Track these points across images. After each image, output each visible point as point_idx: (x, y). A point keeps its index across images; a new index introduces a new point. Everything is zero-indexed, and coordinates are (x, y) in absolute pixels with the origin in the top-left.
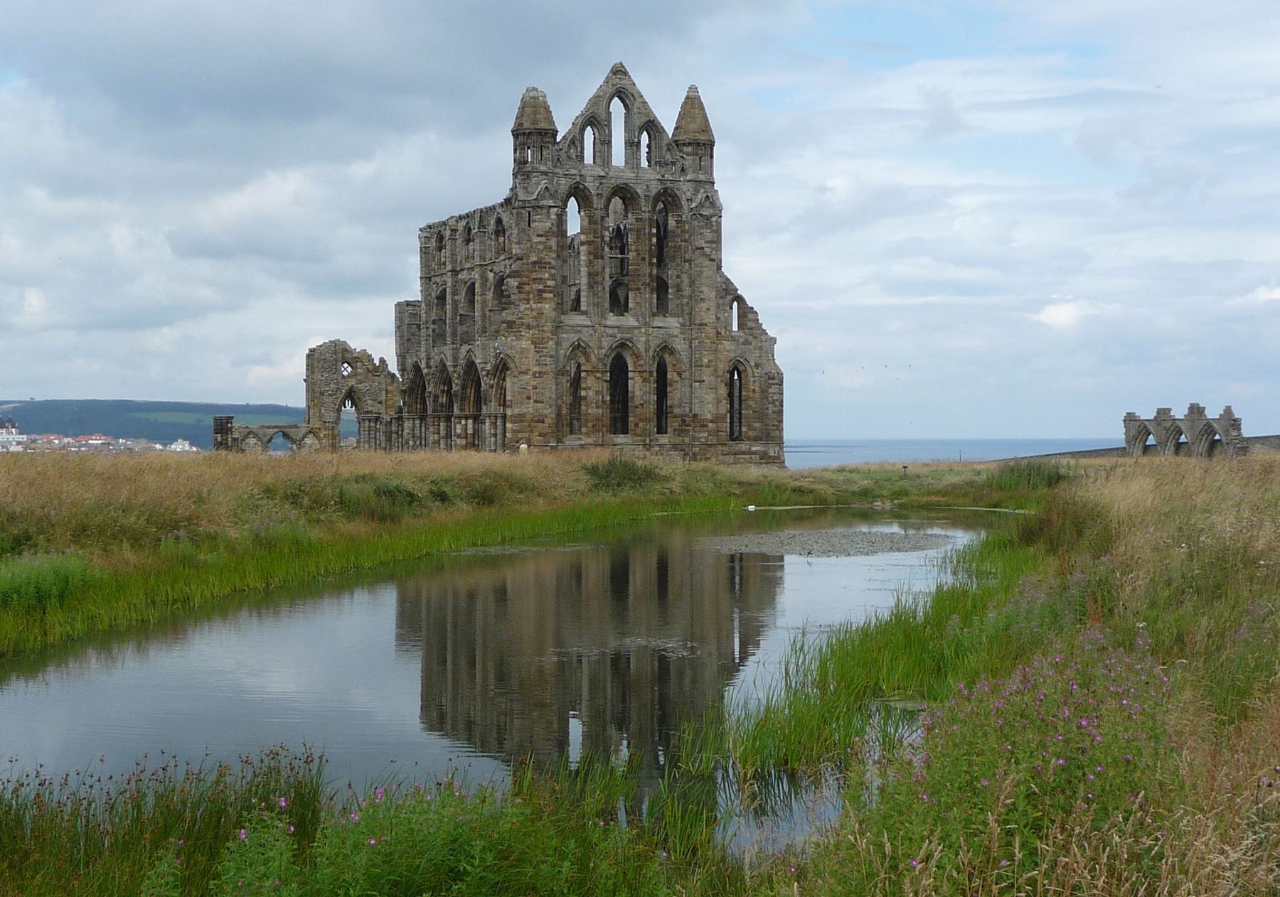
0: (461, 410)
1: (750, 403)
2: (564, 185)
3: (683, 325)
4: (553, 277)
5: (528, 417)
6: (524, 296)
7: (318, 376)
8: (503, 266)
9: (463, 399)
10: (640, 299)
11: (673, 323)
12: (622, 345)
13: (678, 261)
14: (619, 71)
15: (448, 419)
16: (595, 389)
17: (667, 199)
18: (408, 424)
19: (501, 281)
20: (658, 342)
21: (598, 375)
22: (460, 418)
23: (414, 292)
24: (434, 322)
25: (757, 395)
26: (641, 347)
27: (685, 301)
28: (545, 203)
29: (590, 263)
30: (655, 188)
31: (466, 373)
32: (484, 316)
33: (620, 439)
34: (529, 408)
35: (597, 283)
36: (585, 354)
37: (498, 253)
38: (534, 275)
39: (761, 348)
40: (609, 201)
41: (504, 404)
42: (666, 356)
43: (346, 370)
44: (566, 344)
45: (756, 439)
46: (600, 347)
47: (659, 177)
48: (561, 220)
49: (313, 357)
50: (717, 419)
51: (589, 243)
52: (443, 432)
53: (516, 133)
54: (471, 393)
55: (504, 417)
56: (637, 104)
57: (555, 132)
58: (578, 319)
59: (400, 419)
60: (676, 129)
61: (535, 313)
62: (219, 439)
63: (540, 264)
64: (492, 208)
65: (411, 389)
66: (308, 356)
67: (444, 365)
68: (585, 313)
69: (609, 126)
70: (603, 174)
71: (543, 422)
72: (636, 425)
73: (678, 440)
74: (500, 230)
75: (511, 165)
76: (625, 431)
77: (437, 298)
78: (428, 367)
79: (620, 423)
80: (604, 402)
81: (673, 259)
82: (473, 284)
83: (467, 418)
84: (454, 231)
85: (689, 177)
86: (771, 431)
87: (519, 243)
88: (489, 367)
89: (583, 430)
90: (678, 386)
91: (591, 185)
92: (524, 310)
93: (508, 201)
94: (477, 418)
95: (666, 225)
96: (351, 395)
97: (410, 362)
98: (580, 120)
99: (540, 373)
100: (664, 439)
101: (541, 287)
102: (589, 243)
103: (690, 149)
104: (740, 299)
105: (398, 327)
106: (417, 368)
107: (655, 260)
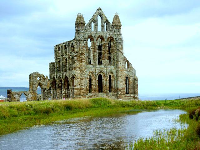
0: (64, 87)
2: (87, 35)
4: (85, 56)
5: (79, 89)
7: (32, 80)
8: (73, 54)
9: (65, 85)
10: (105, 61)
11: (112, 67)
12: (101, 72)
15: (61, 90)
16: (95, 82)
17: (111, 39)
18: (52, 91)
19: (73, 58)
22: (64, 89)
23: (53, 61)
24: (58, 67)
26: (105, 72)
27: (115, 62)
29: (93, 53)
30: (108, 36)
31: (65, 79)
32: (69, 65)
33: (101, 94)
34: (78, 87)
36: (93, 74)
37: (72, 51)
38: (80, 56)
40: (97, 39)
41: (74, 86)
42: (111, 74)
43: (38, 79)
45: (132, 93)
47: (109, 33)
48: (86, 44)
49: (31, 76)
50: (123, 89)
51: (93, 49)
52: (60, 93)
53: (76, 24)
54: (66, 83)
55: (74, 89)
56: (104, 17)
57: (85, 24)
58: (91, 66)
59: (50, 89)
60: (113, 22)
61: (81, 65)
62: (9, 95)
63: (81, 54)
64: (71, 41)
65: (52, 83)
66: (30, 75)
67: (60, 77)
68: (92, 65)
69: (97, 22)
70: (96, 33)
72: (104, 90)
73: (114, 94)
74: (73, 46)
75: (75, 31)
76: (102, 92)
77: (58, 62)
78: (57, 77)
79: (101, 90)
80: (97, 85)
81: (112, 52)
82: (67, 58)
83: (65, 89)
84: (62, 46)
85: (116, 33)
86: (135, 92)
87: (77, 49)
88: (70, 77)
89: (92, 92)
90: (114, 81)
91: (93, 35)
92: (77, 64)
93: (74, 39)
94: (68, 89)
95: (111, 45)
96: (40, 84)
97: (52, 76)
98: (91, 21)
100: (111, 94)
101: (82, 59)
102: (93, 49)
103: (116, 27)
104: (128, 61)
105: (50, 69)
106: (54, 78)
107: (108, 53)
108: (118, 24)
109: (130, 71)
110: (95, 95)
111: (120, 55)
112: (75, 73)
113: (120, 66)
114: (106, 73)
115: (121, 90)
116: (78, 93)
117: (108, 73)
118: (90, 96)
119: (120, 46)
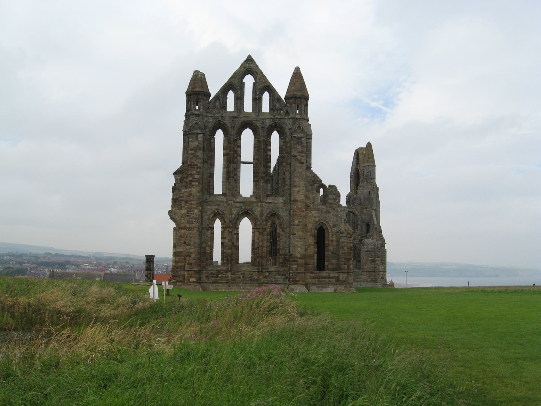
1: (330, 248)
2: (211, 122)
3: (285, 201)
6: (184, 184)
11: (280, 200)
13: (284, 164)
14: (250, 59)
20: (268, 211)
21: (230, 230)
25: (335, 243)
27: (287, 187)
28: (196, 131)
35: (230, 177)
39: (337, 215)
42: (276, 219)
44: (209, 212)
45: (333, 270)
46: (231, 214)
47: (271, 117)
50: (304, 257)
70: (237, 116)
71: (190, 256)
73: (281, 269)
85: (290, 117)
91: (227, 122)
99: (189, 228)
101: (191, 179)
103: (291, 101)
108: (296, 93)
109: (330, 213)
110: (227, 271)
111: (299, 169)
112: (175, 214)
113: (298, 198)
114: (262, 216)
115: (299, 260)
116: (180, 264)
117: (267, 216)
118: (212, 273)
119: (299, 148)
